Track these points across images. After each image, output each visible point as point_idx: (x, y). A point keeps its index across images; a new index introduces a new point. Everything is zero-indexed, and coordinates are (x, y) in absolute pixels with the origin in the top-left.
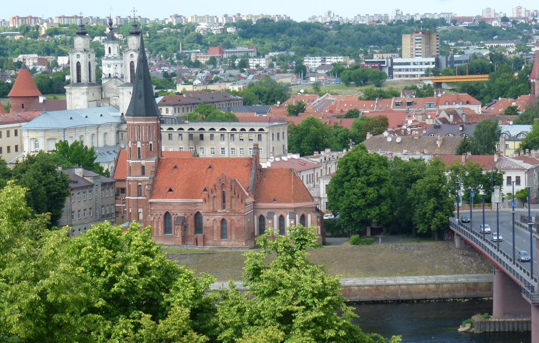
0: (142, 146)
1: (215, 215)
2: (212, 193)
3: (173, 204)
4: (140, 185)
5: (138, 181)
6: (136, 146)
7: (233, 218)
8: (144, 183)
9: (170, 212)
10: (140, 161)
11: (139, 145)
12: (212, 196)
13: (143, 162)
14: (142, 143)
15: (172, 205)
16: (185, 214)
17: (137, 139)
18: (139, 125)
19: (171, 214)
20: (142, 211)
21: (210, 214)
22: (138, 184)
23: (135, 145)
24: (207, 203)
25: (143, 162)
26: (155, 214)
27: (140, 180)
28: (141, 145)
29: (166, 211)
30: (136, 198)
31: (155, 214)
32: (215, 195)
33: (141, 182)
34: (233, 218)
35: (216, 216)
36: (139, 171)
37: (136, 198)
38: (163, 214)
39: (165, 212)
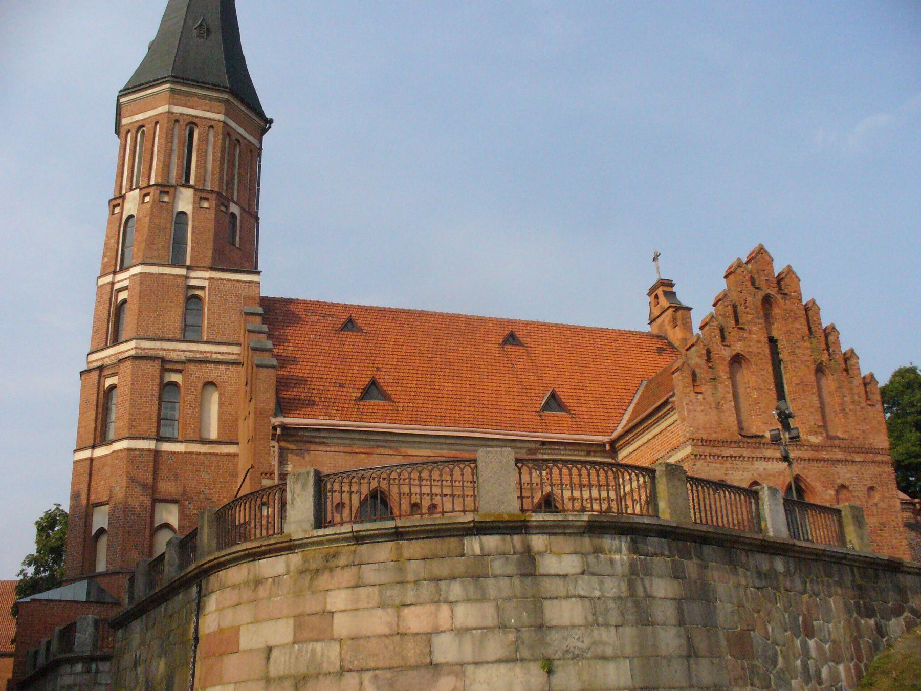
0: (197, 208)
1: (751, 459)
4: (174, 384)
5: (166, 365)
7: (844, 474)
8: (200, 373)
10: (182, 272)
11: (185, 202)
12: (727, 353)
13: (200, 278)
14: (201, 194)
17: (179, 176)
18: (192, 124)
20: (174, 521)
21: (727, 452)
22: (162, 378)
23: (166, 199)
24: (706, 389)
25: (200, 278)
27: (173, 356)
30: (150, 445)
32: (739, 347)
33: (178, 366)
34: (844, 474)
35: (761, 466)
36: (174, 317)
37: (150, 445)
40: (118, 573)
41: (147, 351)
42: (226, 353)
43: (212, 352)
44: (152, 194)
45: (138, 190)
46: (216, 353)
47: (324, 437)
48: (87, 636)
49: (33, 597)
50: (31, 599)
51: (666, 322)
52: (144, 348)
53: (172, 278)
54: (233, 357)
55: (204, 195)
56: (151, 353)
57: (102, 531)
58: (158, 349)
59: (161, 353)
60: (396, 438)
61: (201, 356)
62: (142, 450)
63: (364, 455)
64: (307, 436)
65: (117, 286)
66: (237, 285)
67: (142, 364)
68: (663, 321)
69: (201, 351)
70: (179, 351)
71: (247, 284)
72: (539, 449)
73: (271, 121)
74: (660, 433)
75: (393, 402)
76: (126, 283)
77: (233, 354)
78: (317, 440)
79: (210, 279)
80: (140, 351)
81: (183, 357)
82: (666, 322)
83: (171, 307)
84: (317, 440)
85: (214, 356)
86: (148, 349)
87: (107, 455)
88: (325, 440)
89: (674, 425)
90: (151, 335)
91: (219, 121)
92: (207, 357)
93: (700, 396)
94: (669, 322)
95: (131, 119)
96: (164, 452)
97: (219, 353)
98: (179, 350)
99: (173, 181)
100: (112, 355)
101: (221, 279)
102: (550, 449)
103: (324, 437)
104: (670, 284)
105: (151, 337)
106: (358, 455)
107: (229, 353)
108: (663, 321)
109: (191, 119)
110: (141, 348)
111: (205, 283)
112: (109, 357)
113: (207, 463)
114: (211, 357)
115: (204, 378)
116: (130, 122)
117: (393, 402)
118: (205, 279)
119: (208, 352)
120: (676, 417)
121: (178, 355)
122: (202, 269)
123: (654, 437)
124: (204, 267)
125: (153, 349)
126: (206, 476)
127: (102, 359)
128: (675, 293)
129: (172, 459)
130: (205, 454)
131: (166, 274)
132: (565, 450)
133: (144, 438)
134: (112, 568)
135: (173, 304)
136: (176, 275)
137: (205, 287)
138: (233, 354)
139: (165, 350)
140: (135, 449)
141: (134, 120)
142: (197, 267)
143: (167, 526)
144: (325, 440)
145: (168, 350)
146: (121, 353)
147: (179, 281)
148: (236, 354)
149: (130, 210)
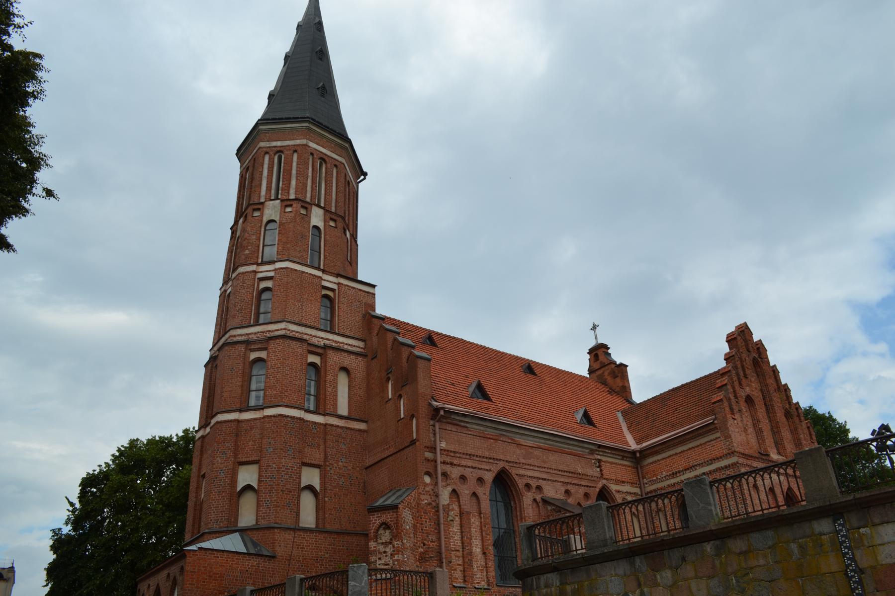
2: (740, 384)
3: (518, 439)
6: (308, 216)
8: (334, 358)
9: (514, 472)
10: (319, 273)
11: (317, 218)
15: (519, 445)
16: (567, 492)
19: (521, 483)
24: (737, 416)
26: (455, 472)
27: (315, 341)
28: (325, 221)
29: (501, 465)
31: (455, 472)
38: (489, 477)
39: (496, 469)
40: (273, 528)
41: (294, 333)
42: (354, 346)
43: (344, 343)
44: (294, 206)
45: (278, 201)
46: (346, 344)
47: (467, 422)
48: (363, 584)
49: (198, 545)
50: (200, 549)
51: (606, 373)
52: (292, 331)
53: (312, 277)
54: (359, 350)
55: (333, 217)
56: (297, 335)
57: (248, 487)
58: (303, 333)
59: (305, 337)
60: (514, 430)
61: (336, 345)
62: (293, 418)
63: (492, 441)
64: (457, 420)
65: (260, 275)
66: (359, 293)
67: (293, 344)
68: (603, 373)
69: (336, 341)
70: (319, 337)
71: (366, 294)
72: (597, 450)
73: (365, 174)
74: (698, 446)
75: (493, 402)
76: (272, 274)
77: (359, 347)
78: (462, 424)
79: (339, 284)
80: (289, 332)
81: (322, 343)
82: (606, 373)
83: (311, 300)
84: (462, 424)
85: (346, 347)
86: (295, 331)
87: (255, 419)
88: (467, 425)
89: (715, 441)
90: (297, 321)
91: (341, 162)
92: (340, 347)
93: (735, 421)
94: (609, 374)
95: (269, 144)
96: (309, 421)
97: (349, 345)
98: (320, 337)
99: (308, 199)
100: (258, 332)
101: (347, 286)
102: (602, 451)
103: (467, 422)
104: (604, 347)
105: (296, 322)
106: (489, 440)
107: (357, 347)
108: (603, 373)
109: (322, 156)
110: (289, 330)
111: (335, 287)
112: (255, 334)
113: (344, 436)
114: (343, 347)
115: (340, 363)
116: (268, 145)
117: (493, 402)
118: (335, 283)
119: (341, 343)
120: (718, 435)
121: (318, 341)
122: (332, 275)
123: (690, 449)
124: (334, 273)
125: (299, 332)
126: (344, 447)
127: (247, 334)
128: (610, 354)
129: (316, 429)
130: (342, 428)
131: (307, 273)
132: (611, 453)
133: (295, 408)
134: (263, 523)
135: (312, 298)
136: (315, 275)
137: (335, 290)
138: (359, 347)
139: (308, 335)
140: (288, 416)
141: (272, 145)
142: (329, 272)
143: (310, 488)
144: (467, 425)
145: (311, 335)
146: (269, 331)
147: (316, 280)
148: (362, 348)
149: (271, 215)
